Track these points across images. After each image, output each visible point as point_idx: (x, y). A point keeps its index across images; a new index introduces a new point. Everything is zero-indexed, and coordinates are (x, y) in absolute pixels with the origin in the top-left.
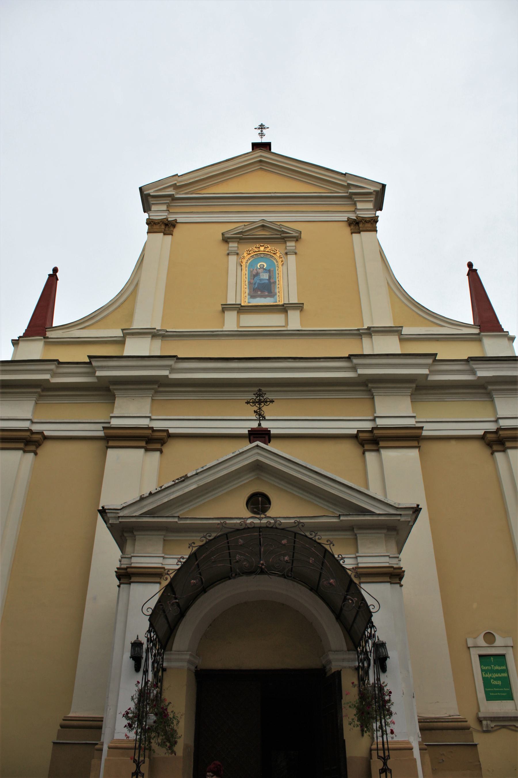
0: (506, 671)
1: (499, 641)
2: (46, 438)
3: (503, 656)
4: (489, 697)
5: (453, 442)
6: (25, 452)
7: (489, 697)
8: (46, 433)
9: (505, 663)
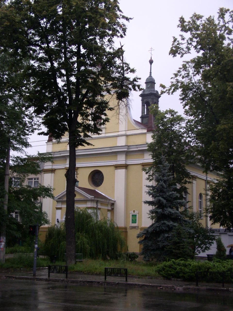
0: (136, 218)
1: (136, 212)
2: (56, 169)
3: (136, 215)
4: (132, 223)
5: (135, 165)
6: (52, 173)
7: (132, 223)
8: (55, 168)
9: (136, 216)
